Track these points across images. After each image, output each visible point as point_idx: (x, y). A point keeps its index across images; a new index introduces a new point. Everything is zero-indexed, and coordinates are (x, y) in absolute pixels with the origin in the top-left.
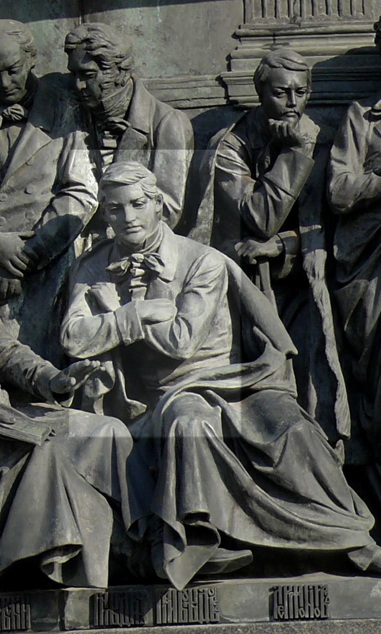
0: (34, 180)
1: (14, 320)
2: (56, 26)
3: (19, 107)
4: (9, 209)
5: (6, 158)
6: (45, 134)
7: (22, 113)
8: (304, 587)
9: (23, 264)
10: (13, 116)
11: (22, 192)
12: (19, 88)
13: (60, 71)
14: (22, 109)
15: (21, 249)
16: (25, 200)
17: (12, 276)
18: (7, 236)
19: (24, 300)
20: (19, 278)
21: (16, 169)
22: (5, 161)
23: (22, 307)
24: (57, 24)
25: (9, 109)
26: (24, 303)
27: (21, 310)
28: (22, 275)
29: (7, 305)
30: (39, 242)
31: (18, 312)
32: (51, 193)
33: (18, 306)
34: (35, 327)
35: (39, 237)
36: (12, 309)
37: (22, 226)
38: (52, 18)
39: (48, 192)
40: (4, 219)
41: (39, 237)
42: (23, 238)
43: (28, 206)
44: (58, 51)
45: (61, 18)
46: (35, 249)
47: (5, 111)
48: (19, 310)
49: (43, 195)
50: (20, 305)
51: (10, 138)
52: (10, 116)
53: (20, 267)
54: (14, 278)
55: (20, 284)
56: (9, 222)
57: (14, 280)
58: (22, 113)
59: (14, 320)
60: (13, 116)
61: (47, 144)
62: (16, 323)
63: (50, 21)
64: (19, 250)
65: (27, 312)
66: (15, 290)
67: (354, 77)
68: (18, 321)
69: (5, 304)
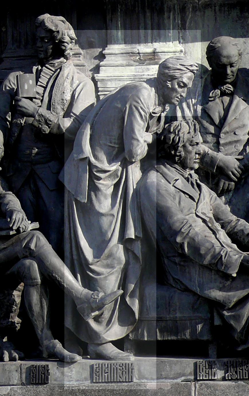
0: (239, 128)
1: (227, 205)
2: (244, 42)
3: (230, 86)
4: (226, 143)
5: (223, 114)
6: (244, 102)
7: (232, 89)
8: (129, 364)
9: (238, 174)
10: (227, 91)
11: (232, 133)
12: (233, 76)
13: (246, 67)
14: (232, 87)
15: (238, 166)
16: (235, 138)
17: (231, 180)
18: (229, 158)
19: (233, 194)
20: (234, 181)
21: (230, 121)
22: (222, 116)
23: (231, 198)
24: (245, 41)
25: (225, 86)
26: (232, 196)
27: (230, 200)
28: (236, 180)
29: (223, 197)
30: (246, 162)
31: (229, 201)
32: (247, 135)
33: (228, 198)
34: (239, 209)
35: (245, 159)
36: (226, 199)
37: (232, 153)
38: (242, 37)
39: (246, 134)
40: (223, 148)
41: (245, 159)
42: (237, 159)
43: (237, 142)
44: (246, 56)
45: (247, 37)
46: (244, 166)
47: (222, 88)
48: (230, 200)
49: (244, 136)
50: (230, 197)
51: (224, 103)
52: (225, 91)
53: (237, 175)
54: (232, 182)
55: (234, 185)
56: (225, 150)
57: (231, 183)
58: (232, 89)
59: (227, 205)
60: (227, 91)
61: (245, 108)
62: (228, 207)
63: (241, 39)
64: (236, 166)
65: (234, 201)
66: (231, 188)
67: (123, 79)
68: (229, 206)
69: (222, 196)
